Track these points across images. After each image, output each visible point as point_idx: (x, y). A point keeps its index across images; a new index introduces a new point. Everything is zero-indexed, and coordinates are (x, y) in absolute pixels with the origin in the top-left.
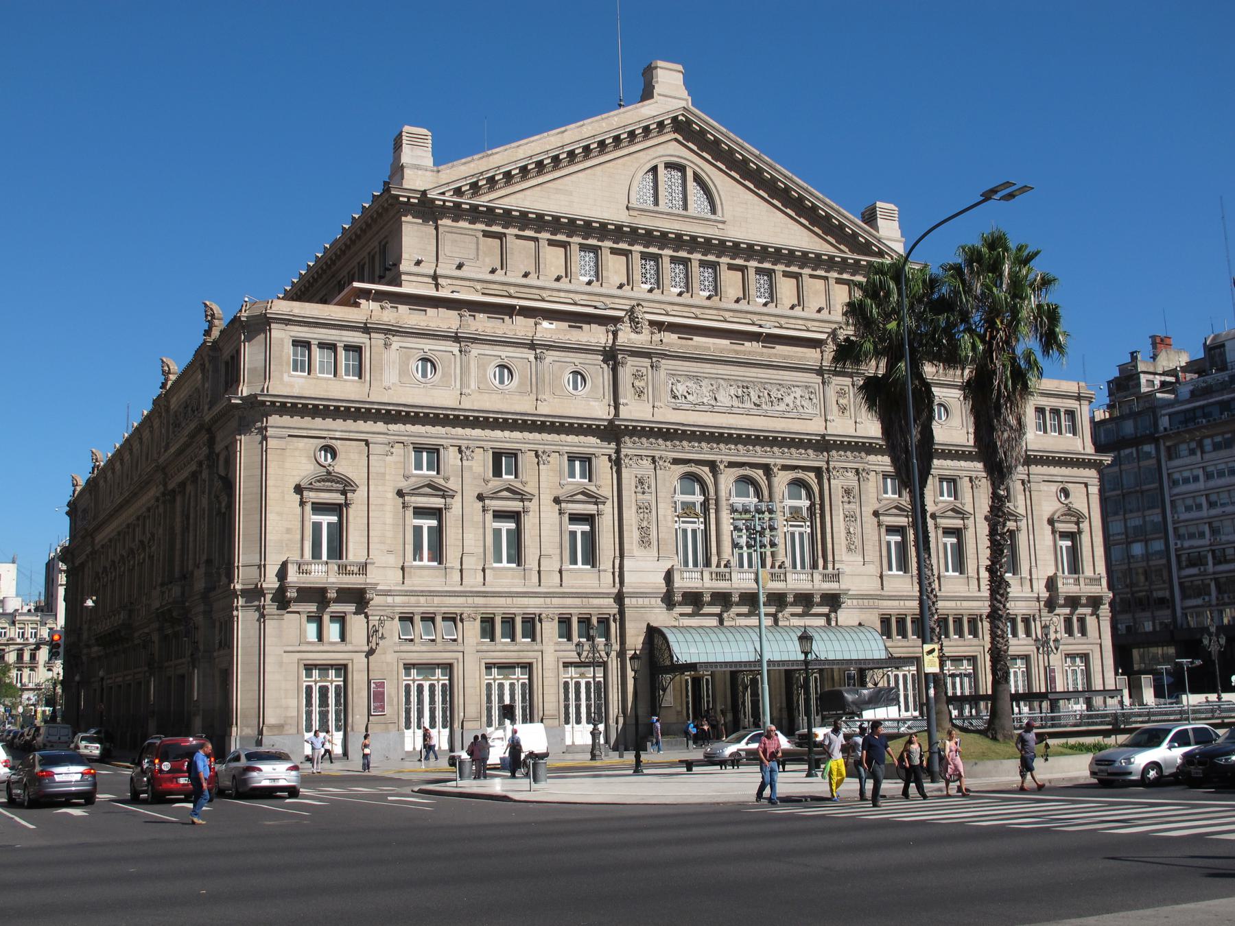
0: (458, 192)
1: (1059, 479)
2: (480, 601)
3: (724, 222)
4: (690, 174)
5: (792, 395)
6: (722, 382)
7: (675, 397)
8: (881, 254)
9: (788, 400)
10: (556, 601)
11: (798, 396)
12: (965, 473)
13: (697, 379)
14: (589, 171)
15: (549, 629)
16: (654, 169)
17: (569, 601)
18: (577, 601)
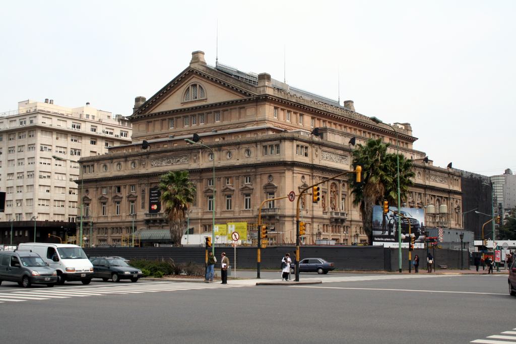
3: (206, 99)
4: (198, 86)
7: (152, 165)
8: (250, 95)
16: (189, 88)
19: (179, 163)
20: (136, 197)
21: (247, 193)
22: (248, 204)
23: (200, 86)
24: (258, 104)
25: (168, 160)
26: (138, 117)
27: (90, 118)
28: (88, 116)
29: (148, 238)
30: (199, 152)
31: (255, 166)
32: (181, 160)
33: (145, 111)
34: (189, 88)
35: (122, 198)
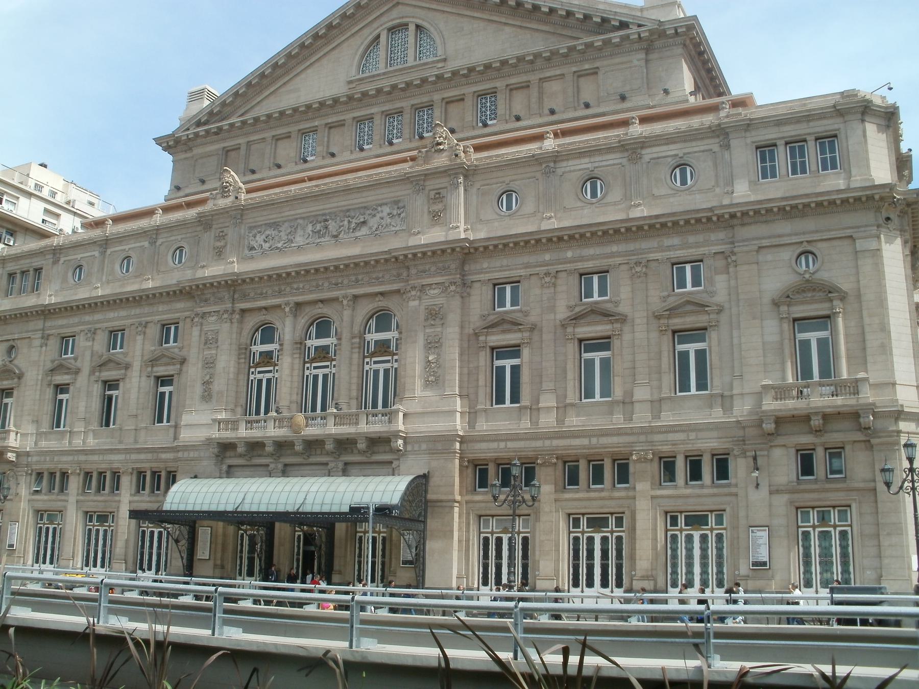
0: (199, 124)
1: (795, 239)
2: (82, 458)
3: (445, 60)
5: (378, 216)
6: (301, 221)
7: (252, 248)
9: (374, 222)
10: (134, 457)
11: (385, 214)
12: (619, 260)
13: (275, 225)
14: (317, 65)
15: (127, 483)
17: (142, 456)
18: (149, 456)
19: (364, 231)
20: (183, 361)
21: (686, 327)
22: (691, 373)
23: (418, 27)
24: (651, 56)
25: (318, 227)
26: (197, 135)
27: (45, 193)
28: (38, 187)
29: (230, 508)
30: (457, 186)
31: (731, 219)
32: (374, 222)
33: (208, 138)
34: (378, 37)
35: (127, 367)
